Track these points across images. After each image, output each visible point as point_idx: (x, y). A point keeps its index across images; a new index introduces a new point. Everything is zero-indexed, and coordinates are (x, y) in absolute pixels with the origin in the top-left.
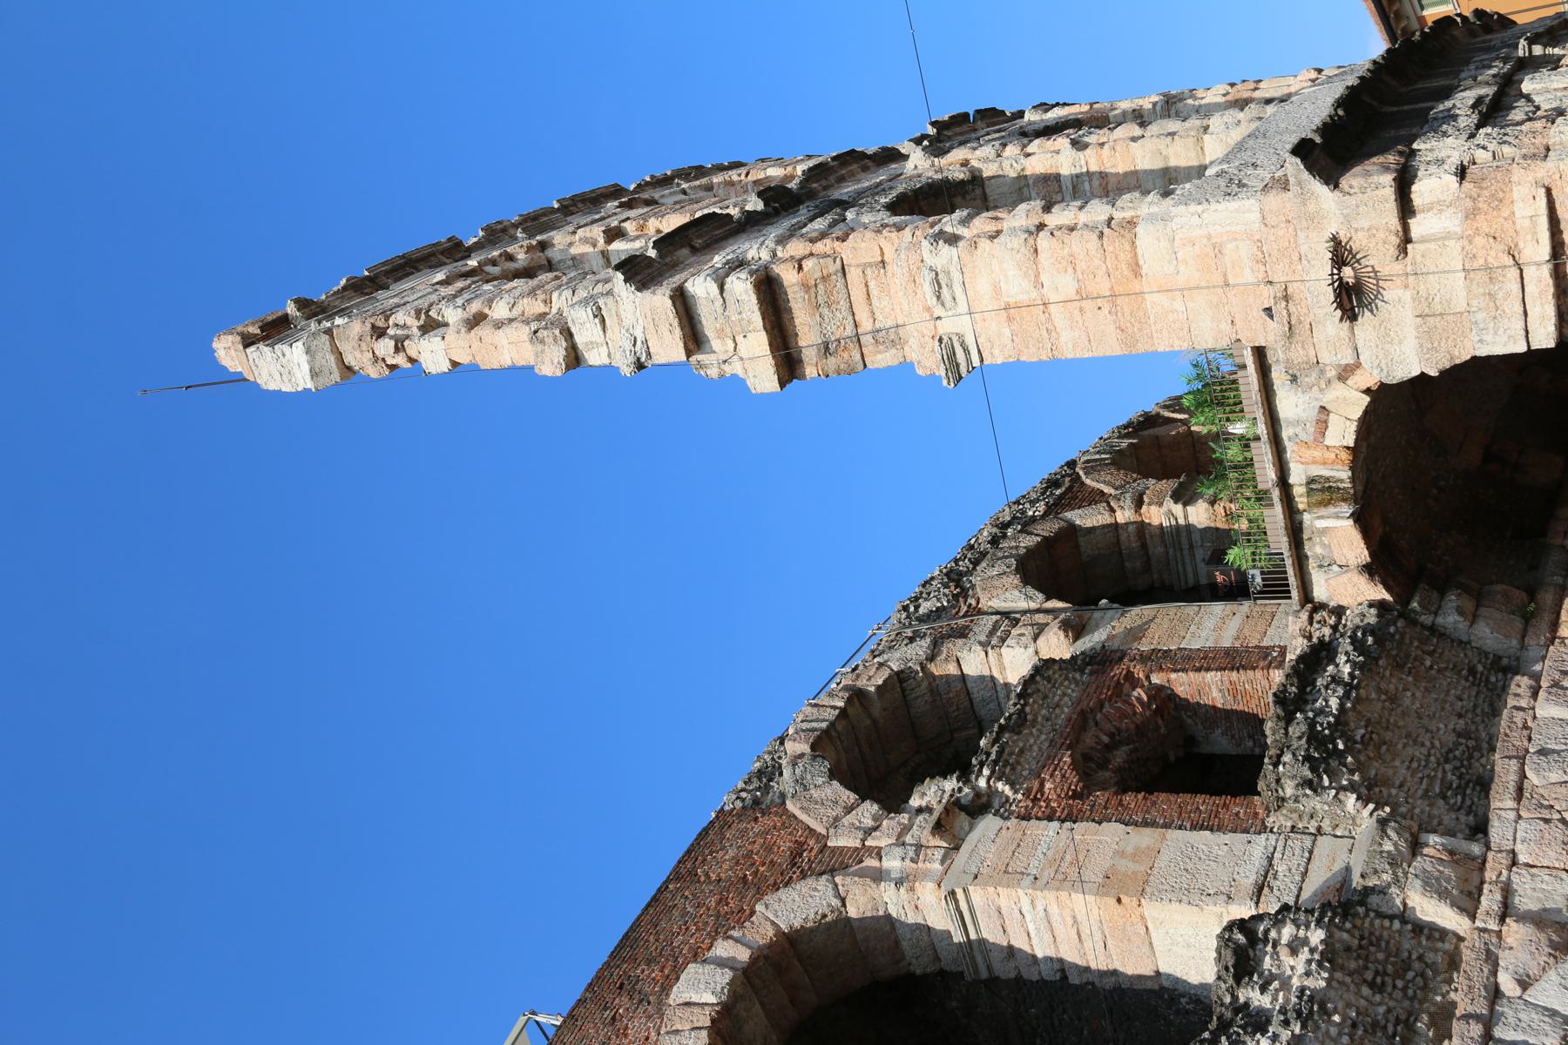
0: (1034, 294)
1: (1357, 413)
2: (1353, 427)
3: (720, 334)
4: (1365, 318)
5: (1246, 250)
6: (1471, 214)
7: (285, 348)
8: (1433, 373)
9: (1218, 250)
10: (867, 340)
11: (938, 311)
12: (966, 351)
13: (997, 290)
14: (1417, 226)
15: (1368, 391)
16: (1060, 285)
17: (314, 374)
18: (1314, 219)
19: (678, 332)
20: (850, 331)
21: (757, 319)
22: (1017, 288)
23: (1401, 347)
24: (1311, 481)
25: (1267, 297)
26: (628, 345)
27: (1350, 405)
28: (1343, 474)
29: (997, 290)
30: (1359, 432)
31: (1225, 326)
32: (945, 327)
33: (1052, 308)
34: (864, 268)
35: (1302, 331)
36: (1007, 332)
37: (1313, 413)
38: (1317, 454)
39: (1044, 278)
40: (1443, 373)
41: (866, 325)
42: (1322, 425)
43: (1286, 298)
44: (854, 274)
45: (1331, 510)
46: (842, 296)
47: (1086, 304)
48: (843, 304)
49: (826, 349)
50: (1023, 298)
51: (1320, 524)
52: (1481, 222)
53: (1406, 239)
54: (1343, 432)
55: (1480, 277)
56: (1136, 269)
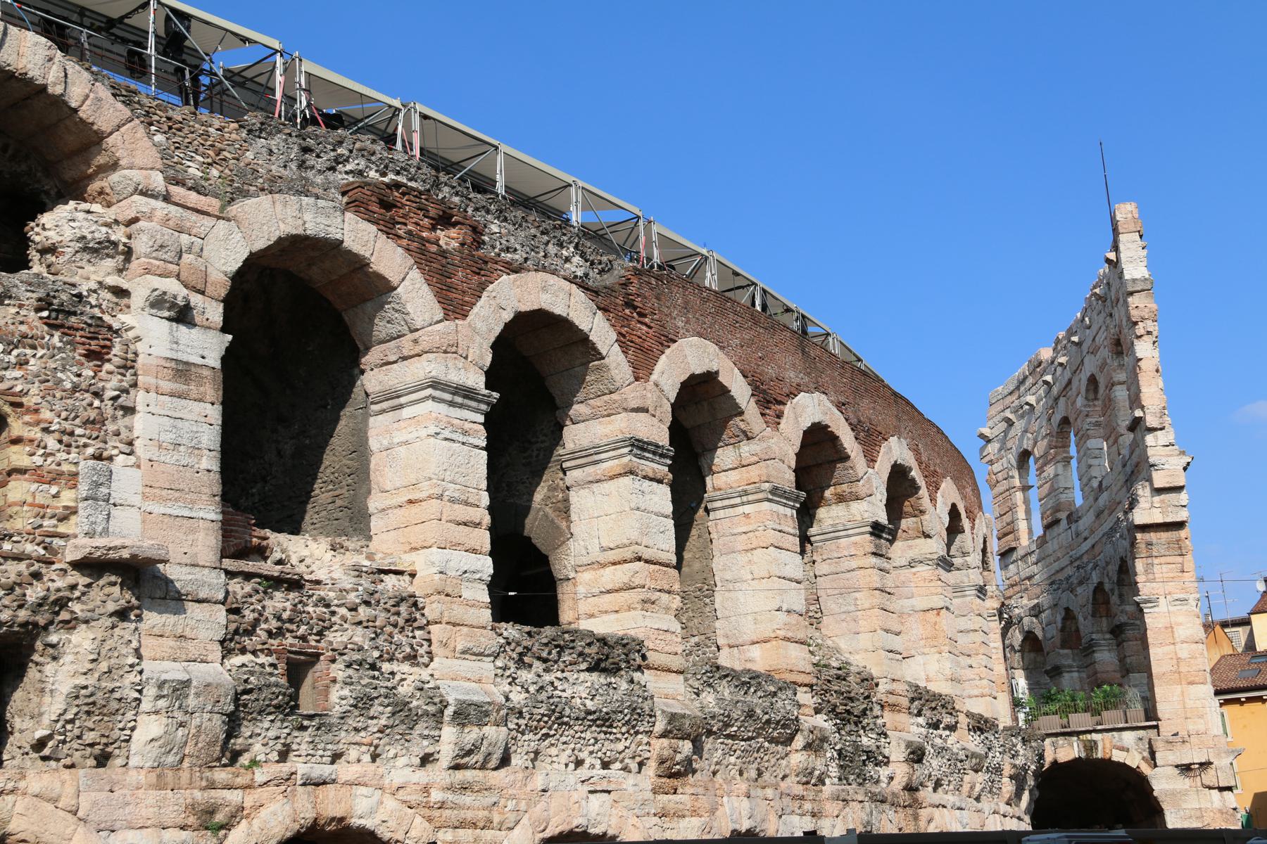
3: (1162, 502)
4: (1177, 771)
5: (1202, 728)
6: (1221, 811)
7: (1145, 263)
8: (1155, 794)
9: (1201, 717)
10: (1150, 560)
13: (1181, 624)
14: (1215, 792)
16: (1184, 651)
17: (1134, 280)
18: (1218, 755)
21: (1169, 520)
22: (1181, 633)
23: (1163, 782)
24: (1095, 742)
25: (1183, 733)
27: (1134, 759)
28: (1100, 755)
29: (1181, 624)
30: (1119, 764)
31: (1167, 716)
32: (1162, 599)
34: (1182, 564)
35: (1170, 746)
37: (1126, 745)
38: (1108, 745)
40: (1155, 798)
41: (1156, 561)
42: (1122, 749)
44: (1179, 559)
47: (1175, 661)
49: (1149, 544)
50: (1176, 635)
51: (1075, 745)
52: (1218, 815)
53: (1210, 788)
54: (1118, 756)
55: (1198, 814)
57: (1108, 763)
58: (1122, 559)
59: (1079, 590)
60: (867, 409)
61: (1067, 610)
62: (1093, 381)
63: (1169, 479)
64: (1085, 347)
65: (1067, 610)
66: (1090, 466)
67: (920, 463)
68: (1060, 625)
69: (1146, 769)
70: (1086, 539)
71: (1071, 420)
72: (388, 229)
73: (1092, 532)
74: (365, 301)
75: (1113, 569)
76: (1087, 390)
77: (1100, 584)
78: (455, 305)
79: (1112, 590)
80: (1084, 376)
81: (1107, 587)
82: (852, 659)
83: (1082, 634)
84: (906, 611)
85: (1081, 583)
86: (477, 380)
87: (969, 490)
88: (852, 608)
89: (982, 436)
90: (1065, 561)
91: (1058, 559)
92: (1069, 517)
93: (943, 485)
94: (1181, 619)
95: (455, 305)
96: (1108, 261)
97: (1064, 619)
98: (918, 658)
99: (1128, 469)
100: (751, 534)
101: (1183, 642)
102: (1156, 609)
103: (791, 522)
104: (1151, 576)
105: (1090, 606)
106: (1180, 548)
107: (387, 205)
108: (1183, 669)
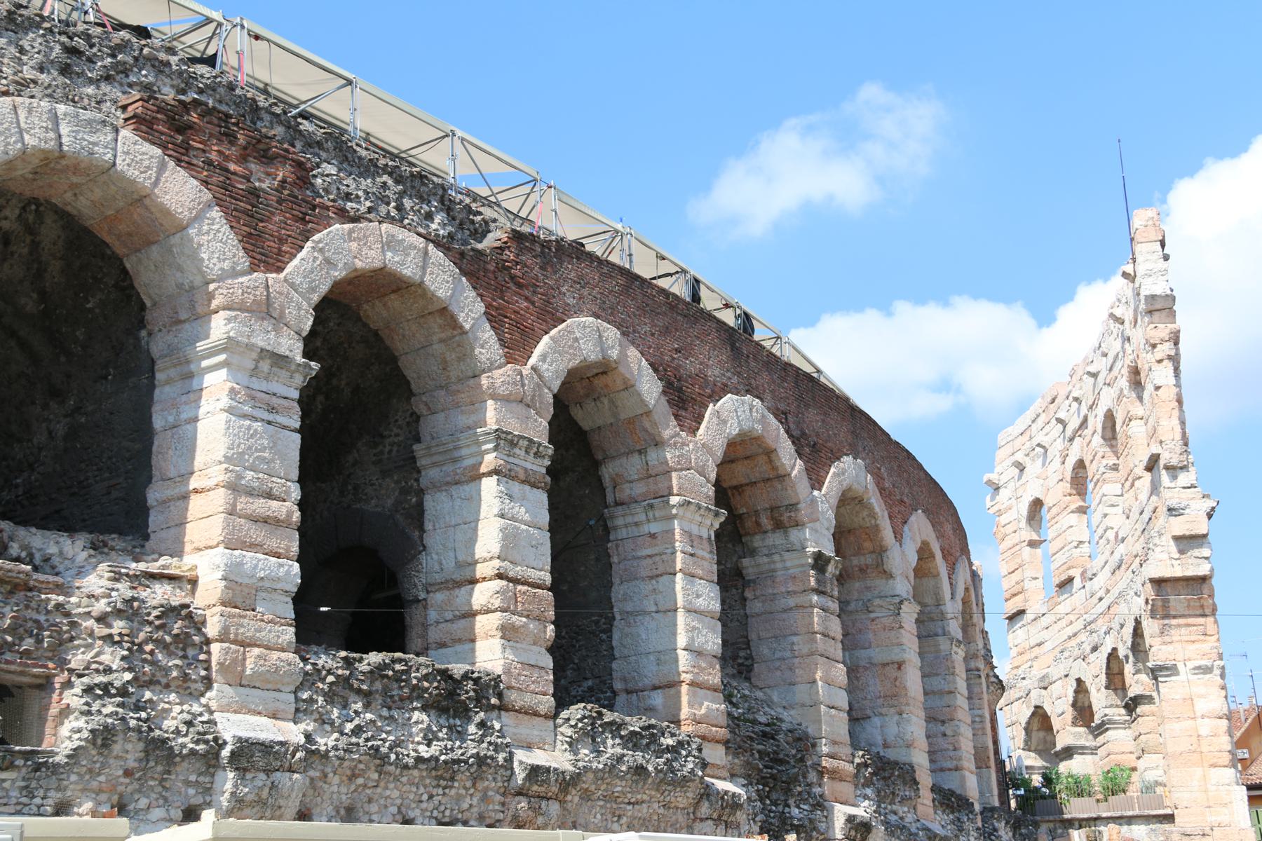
0: (1199, 714)
5: (1225, 819)
10: (1166, 622)
11: (1191, 665)
13: (1200, 696)
16: (1205, 727)
19: (1188, 533)
20: (1173, 613)
21: (1189, 573)
22: (1201, 706)
29: (1200, 696)
32: (1180, 666)
33: (1191, 722)
39: (1207, 720)
41: (1174, 622)
47: (1194, 739)
56: (1214, 766)
58: (1136, 619)
59: (1092, 657)
60: (813, 419)
61: (1079, 681)
62: (1110, 417)
63: (1188, 526)
64: (1101, 378)
65: (1079, 681)
66: (1105, 515)
67: (882, 490)
68: (1071, 699)
70: (1101, 599)
71: (1087, 463)
72: (182, 155)
73: (1108, 591)
74: (149, 243)
75: (1128, 630)
76: (1104, 428)
77: (1115, 649)
78: (265, 252)
79: (1127, 657)
80: (1101, 411)
81: (1122, 652)
82: (784, 715)
83: (1095, 709)
84: (862, 663)
85: (1095, 649)
86: (291, 346)
87: (948, 528)
88: (788, 654)
89: (989, 483)
90: (1079, 625)
91: (1071, 623)
92: (1083, 574)
93: (913, 519)
95: (265, 252)
96: (1125, 275)
97: (1076, 692)
99: (1146, 516)
100: (657, 558)
102: (1173, 678)
103: (706, 545)
104: (1167, 639)
105: (1104, 676)
106: (1202, 607)
107: (184, 128)
108: (1205, 748)
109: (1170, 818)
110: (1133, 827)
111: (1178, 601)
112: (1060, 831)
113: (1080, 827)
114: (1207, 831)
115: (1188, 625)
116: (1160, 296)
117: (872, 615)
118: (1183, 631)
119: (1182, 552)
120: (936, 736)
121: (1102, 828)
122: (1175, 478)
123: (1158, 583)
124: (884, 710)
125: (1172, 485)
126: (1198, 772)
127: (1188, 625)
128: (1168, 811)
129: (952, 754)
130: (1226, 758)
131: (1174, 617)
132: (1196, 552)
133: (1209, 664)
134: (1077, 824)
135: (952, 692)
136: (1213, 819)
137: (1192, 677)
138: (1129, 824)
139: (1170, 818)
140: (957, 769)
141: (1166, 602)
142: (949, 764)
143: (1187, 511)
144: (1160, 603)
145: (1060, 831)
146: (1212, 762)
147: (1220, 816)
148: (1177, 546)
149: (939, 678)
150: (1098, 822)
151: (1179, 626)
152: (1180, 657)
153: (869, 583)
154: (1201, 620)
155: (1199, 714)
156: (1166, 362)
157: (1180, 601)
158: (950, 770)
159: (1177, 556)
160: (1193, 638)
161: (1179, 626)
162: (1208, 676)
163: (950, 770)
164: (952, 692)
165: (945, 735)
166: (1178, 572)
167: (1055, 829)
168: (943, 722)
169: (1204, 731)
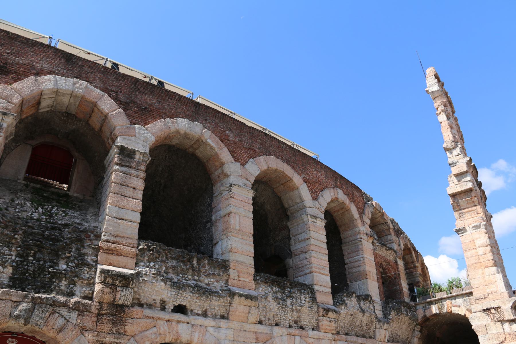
0: (477, 246)
1: (460, 313)
2: (456, 312)
10: (461, 212)
11: (471, 226)
12: (462, 233)
13: (477, 239)
15: (465, 315)
16: (481, 251)
20: (463, 208)
21: (464, 188)
22: (478, 243)
26: (455, 162)
27: (462, 311)
29: (477, 239)
30: (455, 314)
32: (467, 228)
33: (474, 250)
36: (468, 241)
38: (449, 305)
39: (481, 248)
42: (456, 306)
43: (485, 298)
45: (437, 309)
46: (470, 206)
47: (477, 257)
48: (468, 206)
50: (476, 244)
54: (455, 310)
57: (450, 314)
63: (459, 169)
69: (468, 315)
84: (218, 218)
94: (478, 236)
98: (220, 243)
101: (479, 247)
102: (465, 234)
104: (462, 219)
106: (473, 202)
108: (482, 260)
109: (471, 294)
110: (457, 300)
111: (462, 202)
112: (427, 307)
113: (436, 304)
114: (486, 296)
115: (470, 211)
116: (435, 91)
117: (222, 195)
118: (468, 214)
119: (459, 181)
120: (303, 260)
121: (444, 303)
122: (451, 153)
123: (453, 196)
124: (222, 237)
125: (451, 156)
126: (480, 271)
127: (470, 211)
128: (470, 291)
129: (308, 266)
130: (491, 263)
131: (463, 209)
132: (465, 180)
133: (478, 224)
134: (434, 302)
135: (308, 239)
136: (489, 290)
137: (472, 231)
138: (455, 299)
139: (471, 294)
140: (311, 272)
141: (458, 203)
142: (308, 271)
143: (457, 164)
144: (455, 204)
145: (427, 307)
146: (485, 265)
147: (492, 288)
148: (457, 179)
149: (304, 234)
150: (442, 300)
151: (466, 212)
152: (466, 224)
153: (222, 182)
154: (475, 208)
155: (477, 246)
156: (442, 113)
157: (463, 202)
158: (308, 273)
159: (457, 183)
160: (473, 216)
161: (466, 212)
162: (479, 230)
163: (308, 273)
164: (308, 239)
165: (306, 258)
166: (459, 189)
167: (426, 306)
168: (306, 252)
169: (480, 253)
